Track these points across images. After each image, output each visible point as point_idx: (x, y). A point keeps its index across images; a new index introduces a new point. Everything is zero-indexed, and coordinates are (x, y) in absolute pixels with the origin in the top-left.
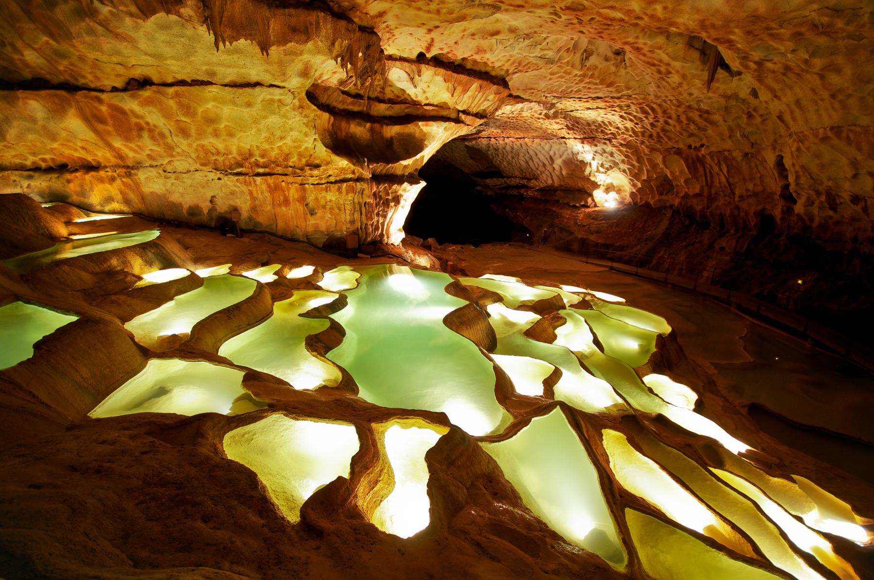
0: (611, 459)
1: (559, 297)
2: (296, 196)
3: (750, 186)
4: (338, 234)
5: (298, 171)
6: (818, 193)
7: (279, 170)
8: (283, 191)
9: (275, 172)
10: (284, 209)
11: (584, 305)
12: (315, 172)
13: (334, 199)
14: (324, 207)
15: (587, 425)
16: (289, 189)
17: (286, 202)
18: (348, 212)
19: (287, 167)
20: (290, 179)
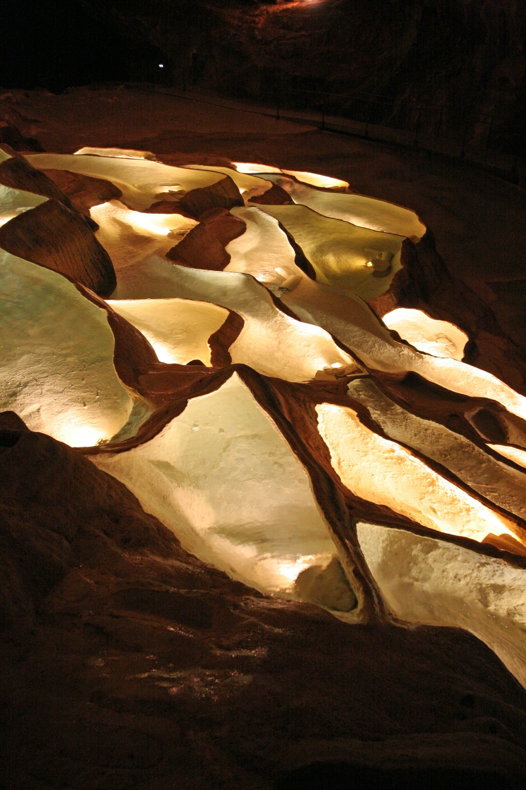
0: (332, 453)
1: (229, 183)
11: (275, 195)
15: (288, 403)
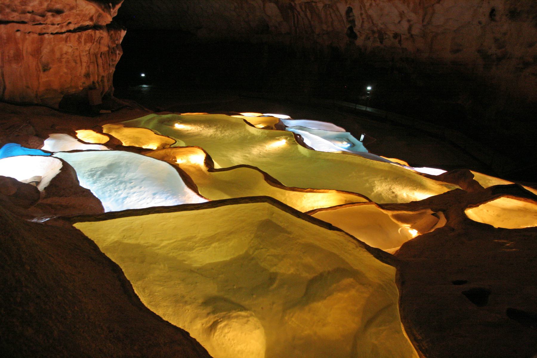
2: (29, 50)
3: (325, 27)
4: (72, 91)
5: (38, 18)
6: (373, 32)
7: (15, 16)
8: (17, 43)
9: (10, 18)
10: (14, 66)
12: (58, 19)
13: (70, 50)
14: (60, 60)
16: (24, 40)
17: (18, 57)
18: (84, 65)
19: (24, 12)
20: (28, 28)
